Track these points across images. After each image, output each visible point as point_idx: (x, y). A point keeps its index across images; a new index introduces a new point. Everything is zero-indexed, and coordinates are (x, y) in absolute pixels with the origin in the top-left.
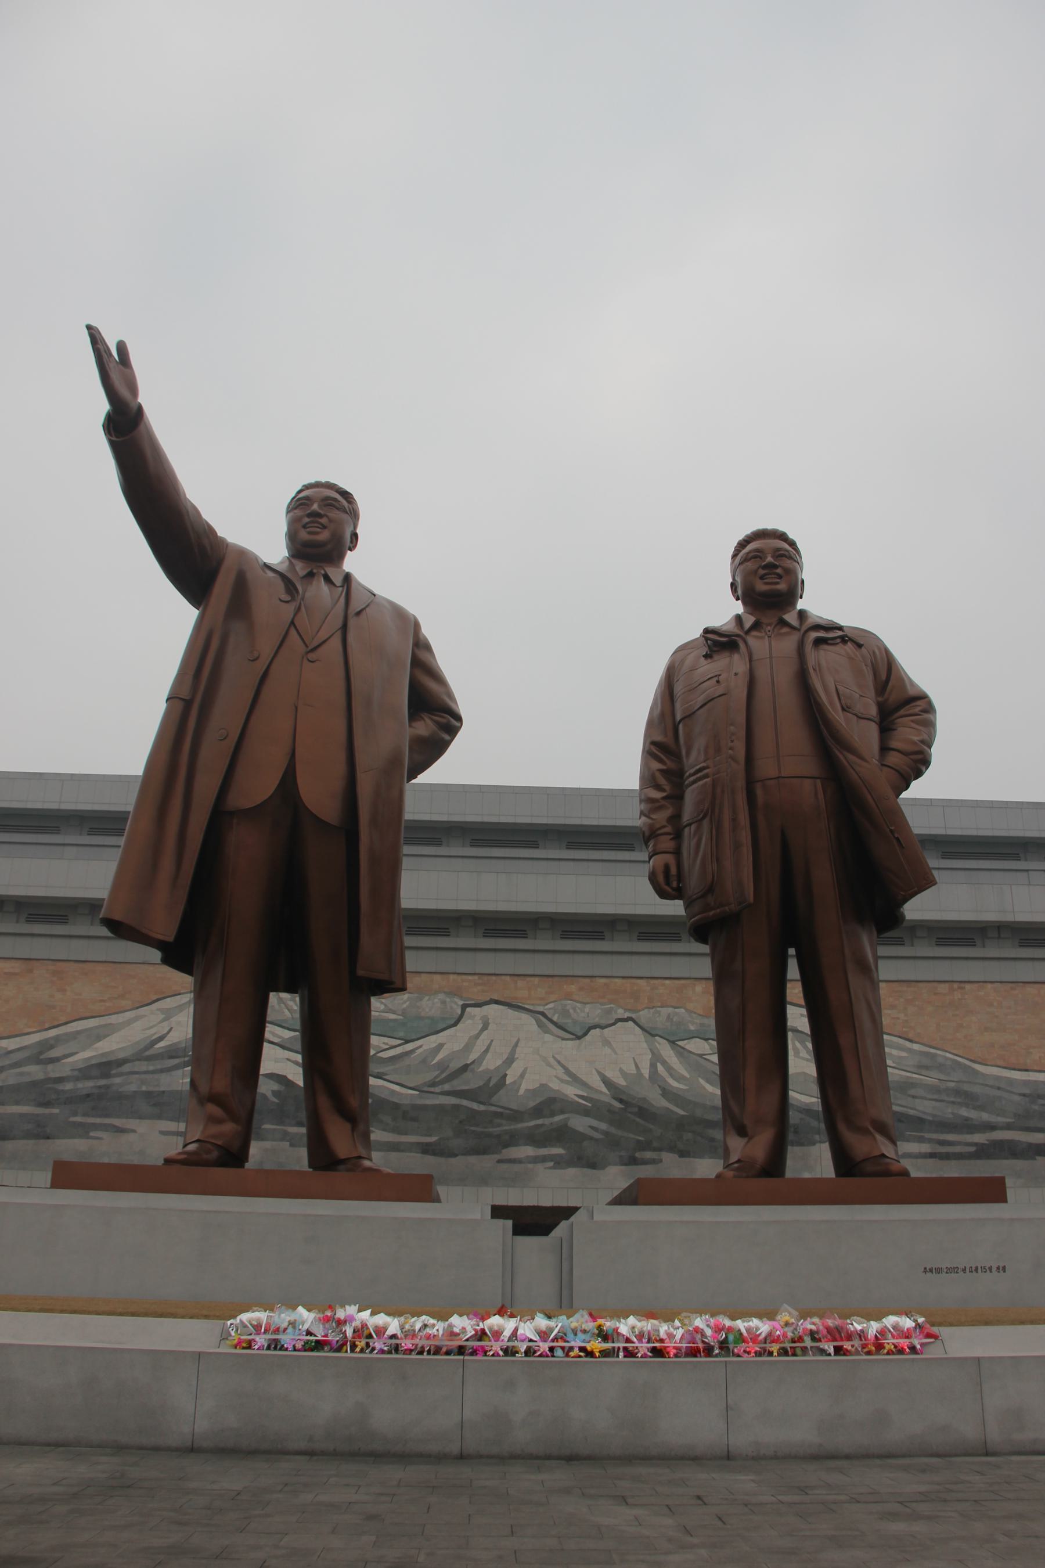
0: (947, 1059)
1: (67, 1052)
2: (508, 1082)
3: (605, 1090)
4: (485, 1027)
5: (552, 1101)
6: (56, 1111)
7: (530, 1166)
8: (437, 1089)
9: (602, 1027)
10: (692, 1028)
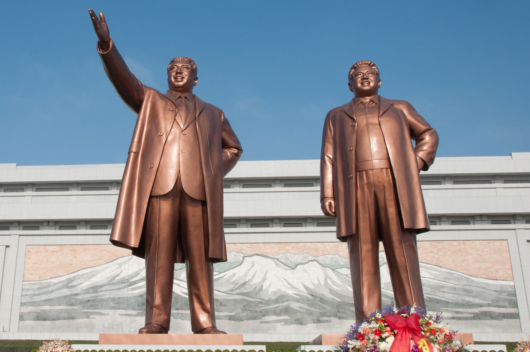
0: (458, 275)
2: (264, 288)
3: (305, 291)
4: (253, 265)
5: (283, 296)
6: (76, 307)
7: (274, 324)
8: (234, 293)
9: (303, 264)
10: (342, 263)
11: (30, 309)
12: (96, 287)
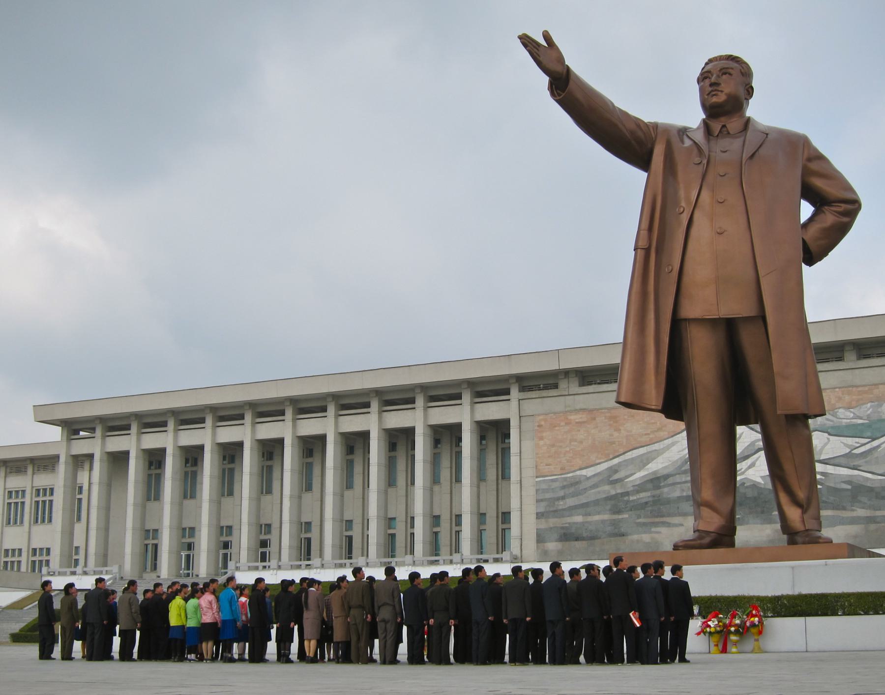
1: (628, 473)
6: (626, 516)
11: (553, 522)
12: (658, 478)
